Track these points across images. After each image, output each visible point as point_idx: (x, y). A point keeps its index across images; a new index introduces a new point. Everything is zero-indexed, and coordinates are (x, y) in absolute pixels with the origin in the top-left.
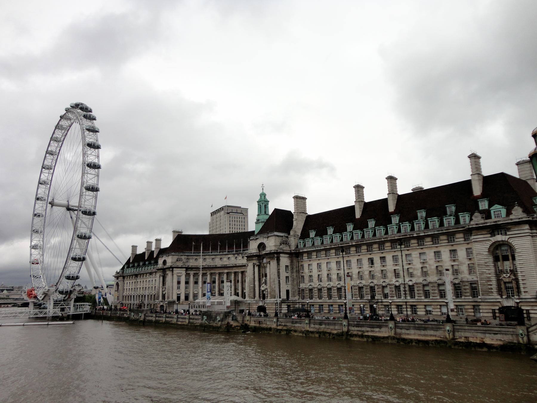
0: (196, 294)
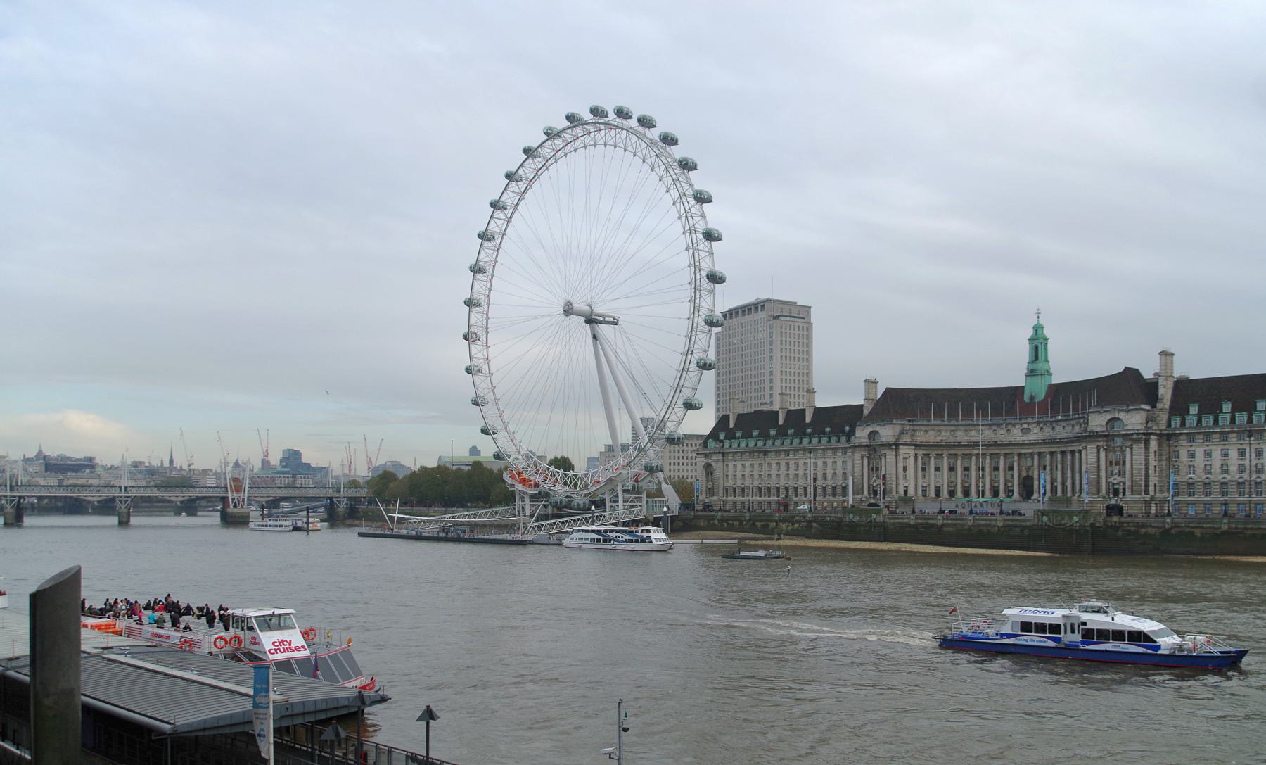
0: (923, 487)
